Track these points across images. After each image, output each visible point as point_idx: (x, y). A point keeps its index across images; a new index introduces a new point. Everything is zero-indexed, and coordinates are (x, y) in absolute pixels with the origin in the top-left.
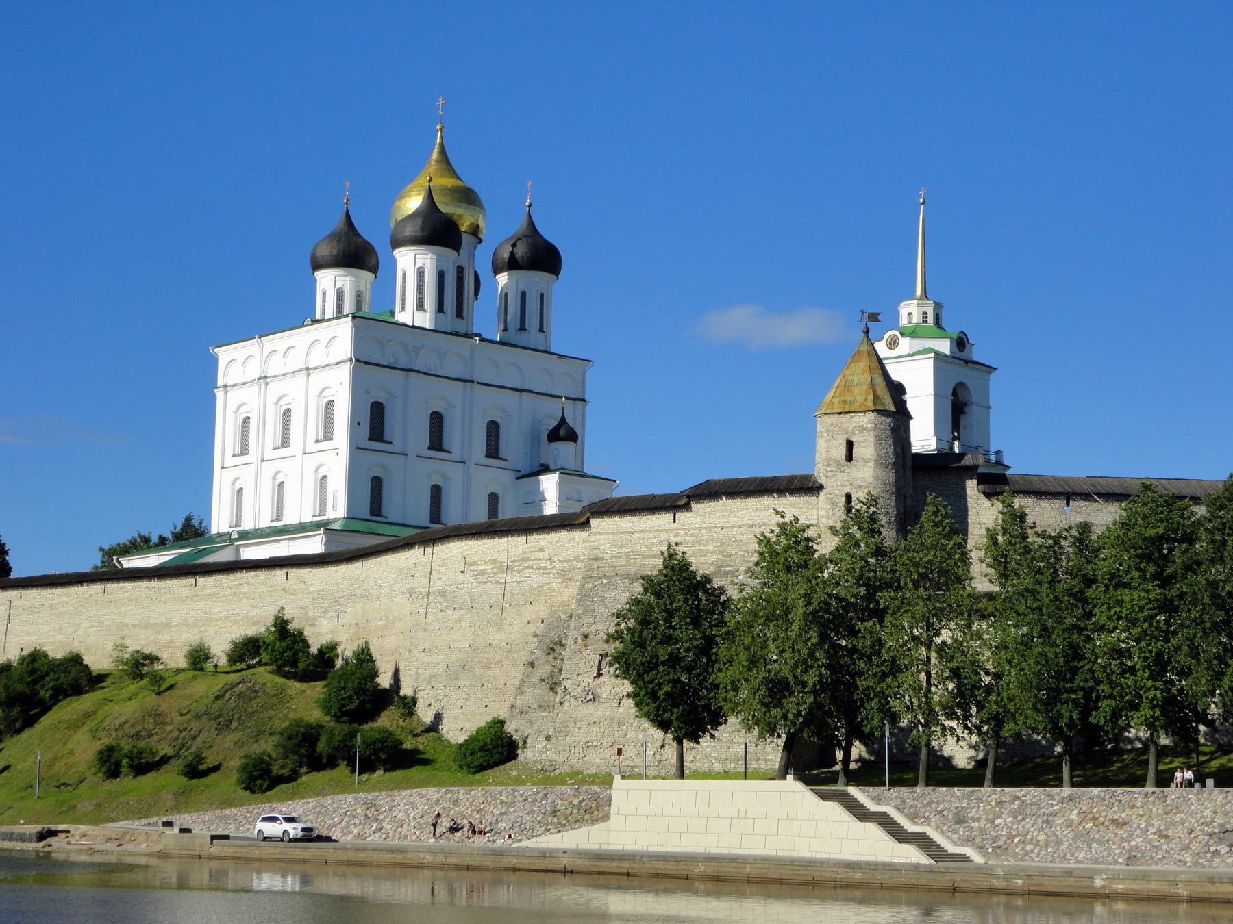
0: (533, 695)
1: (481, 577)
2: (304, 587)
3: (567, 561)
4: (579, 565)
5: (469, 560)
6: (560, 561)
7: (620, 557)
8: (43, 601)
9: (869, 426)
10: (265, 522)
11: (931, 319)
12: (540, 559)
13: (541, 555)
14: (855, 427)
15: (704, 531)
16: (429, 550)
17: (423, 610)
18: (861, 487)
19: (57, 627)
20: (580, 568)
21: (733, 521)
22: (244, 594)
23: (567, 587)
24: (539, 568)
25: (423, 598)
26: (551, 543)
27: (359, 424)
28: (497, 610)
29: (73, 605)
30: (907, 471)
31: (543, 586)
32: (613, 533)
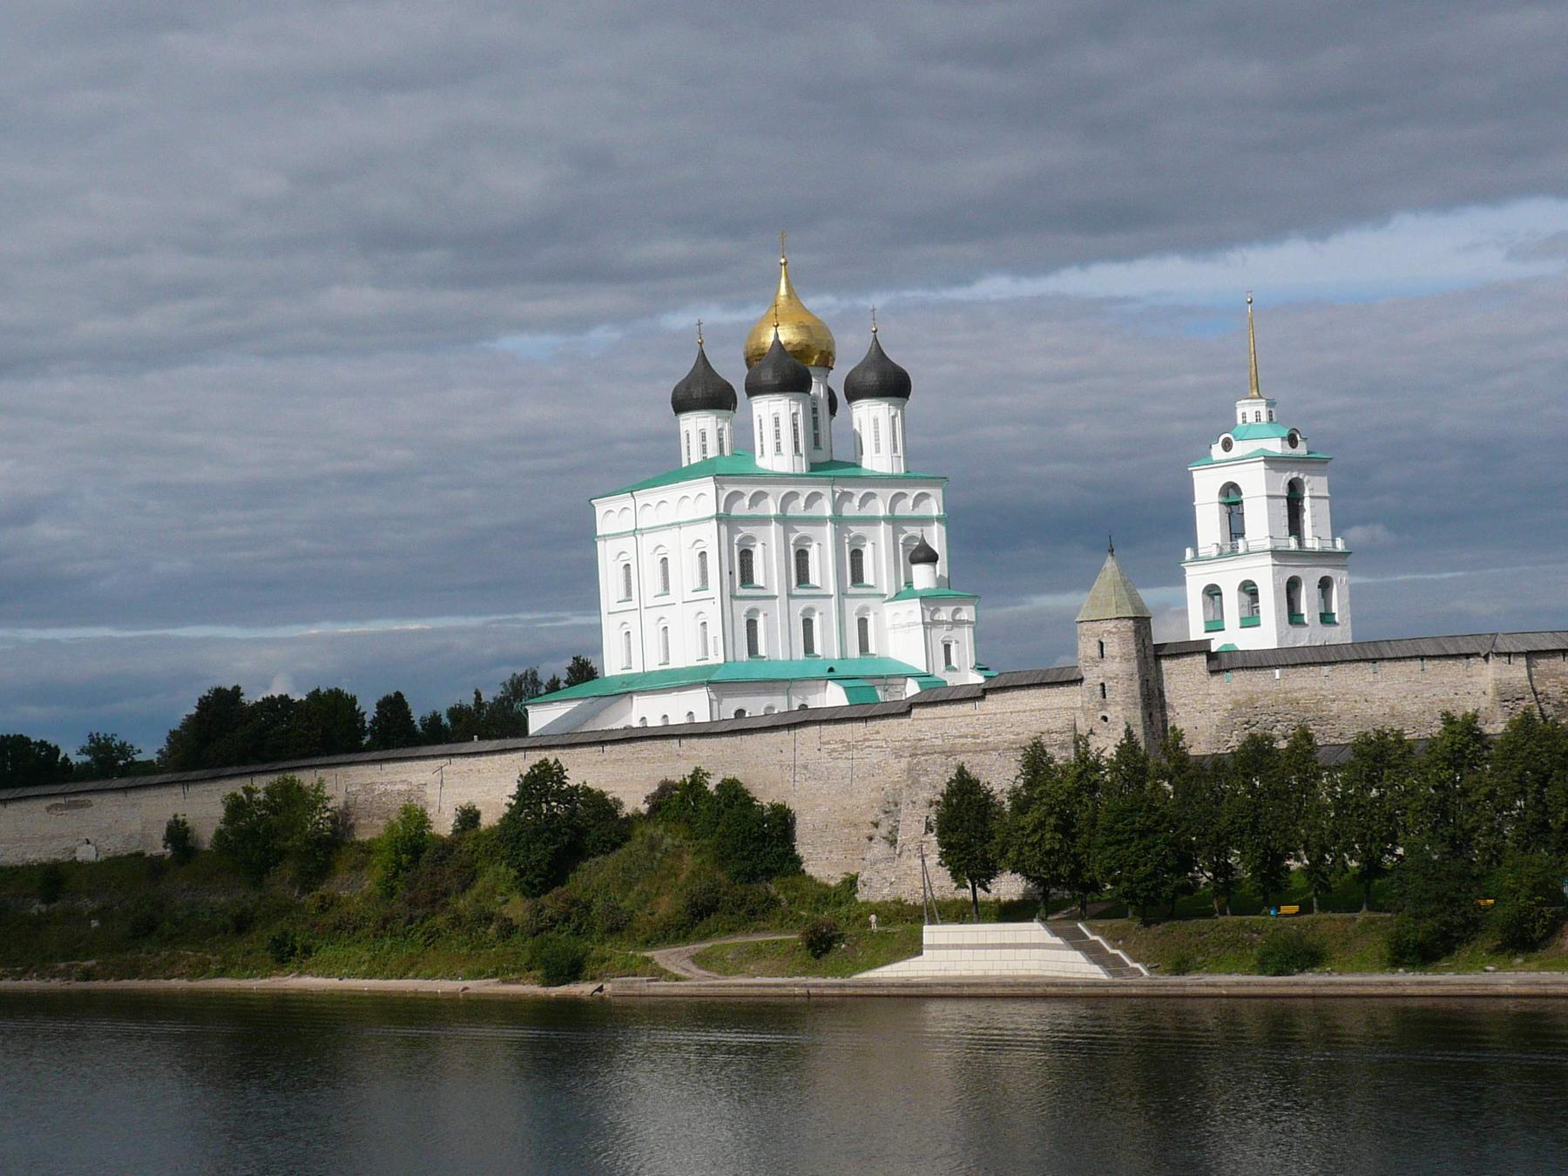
0: (880, 849)
1: (834, 754)
2: (695, 753)
3: (898, 741)
4: (907, 744)
5: (823, 740)
6: (893, 741)
7: (937, 738)
8: (472, 767)
9: (1114, 630)
10: (653, 665)
11: (1264, 418)
12: (876, 740)
13: (877, 736)
14: (1104, 631)
15: (998, 716)
16: (792, 732)
17: (792, 780)
18: (1111, 678)
19: (486, 789)
20: (908, 747)
21: (1019, 707)
22: (645, 758)
23: (899, 762)
24: (877, 747)
25: (791, 770)
26: (884, 727)
27: (730, 573)
28: (847, 781)
29: (498, 769)
30: (1149, 659)
31: (881, 762)
32: (931, 719)
